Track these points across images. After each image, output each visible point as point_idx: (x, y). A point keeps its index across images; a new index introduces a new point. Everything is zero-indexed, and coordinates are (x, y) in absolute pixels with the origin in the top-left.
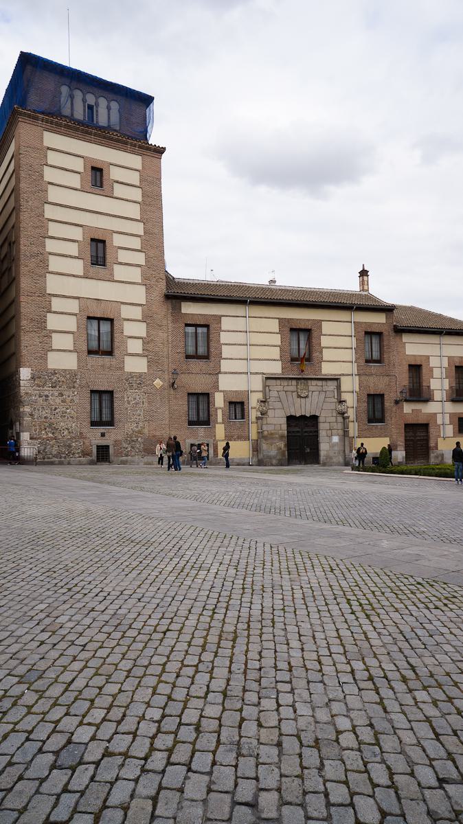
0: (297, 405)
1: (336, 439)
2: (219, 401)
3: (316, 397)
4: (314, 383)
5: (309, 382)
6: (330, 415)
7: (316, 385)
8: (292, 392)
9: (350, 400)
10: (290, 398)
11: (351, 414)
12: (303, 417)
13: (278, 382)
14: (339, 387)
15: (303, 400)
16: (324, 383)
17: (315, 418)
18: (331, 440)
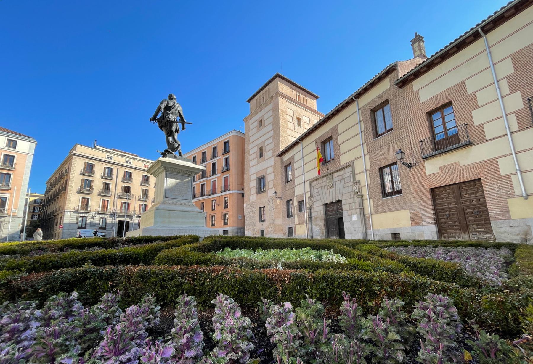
0: (328, 195)
1: (355, 218)
2: (295, 202)
3: (338, 185)
4: (337, 174)
5: (334, 175)
6: (349, 197)
7: (338, 176)
8: (325, 186)
9: (364, 179)
10: (324, 192)
11: (365, 192)
12: (332, 203)
13: (317, 181)
14: (353, 171)
15: (331, 190)
16: (343, 171)
17: (339, 201)
18: (351, 218)
